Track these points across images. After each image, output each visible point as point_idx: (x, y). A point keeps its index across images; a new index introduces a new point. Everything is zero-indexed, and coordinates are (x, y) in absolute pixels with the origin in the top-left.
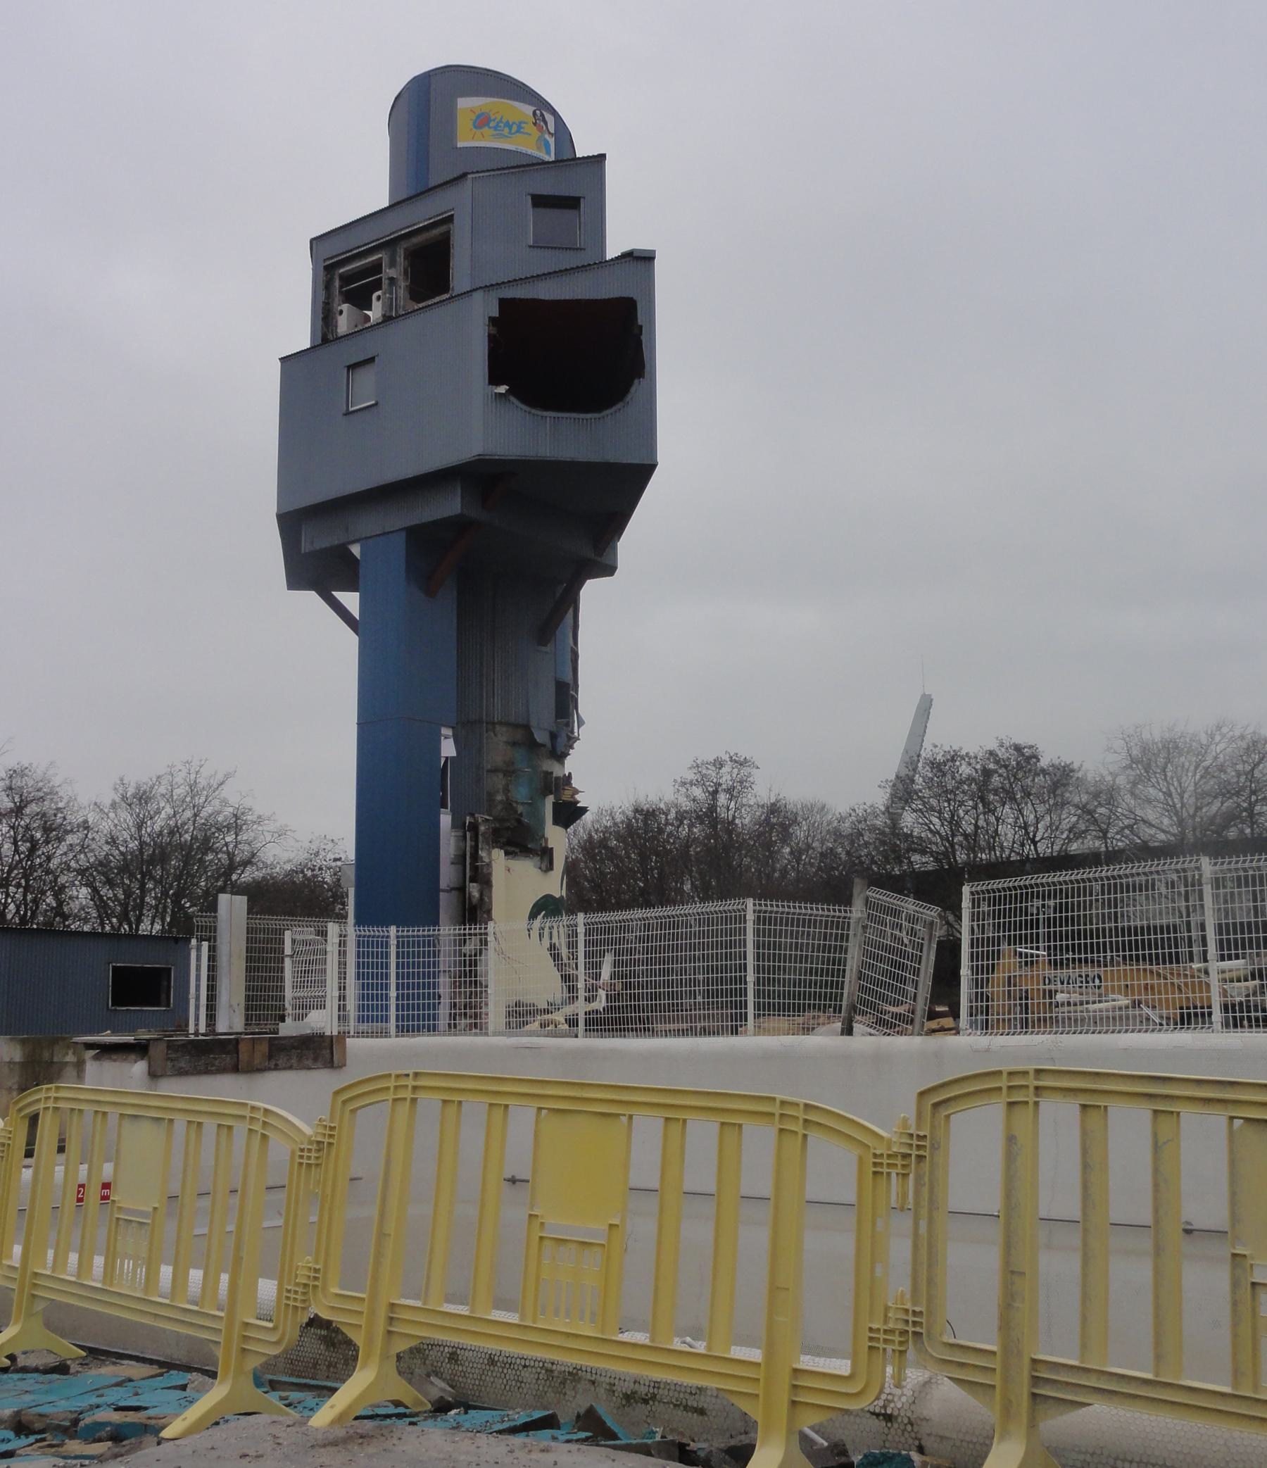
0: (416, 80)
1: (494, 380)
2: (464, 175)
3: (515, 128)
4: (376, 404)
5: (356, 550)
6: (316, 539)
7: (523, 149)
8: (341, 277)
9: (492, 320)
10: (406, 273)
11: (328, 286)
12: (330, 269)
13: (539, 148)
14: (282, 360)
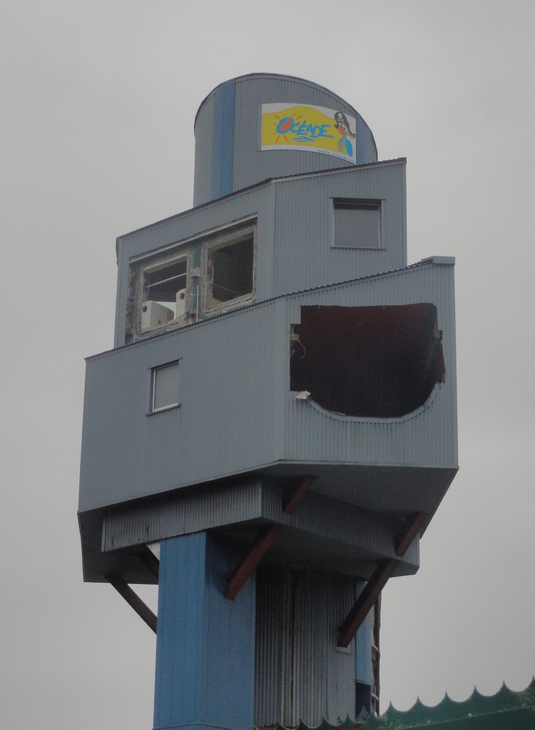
0: (222, 88)
1: (296, 386)
2: (269, 180)
3: (317, 131)
4: (179, 406)
5: (156, 550)
6: (117, 538)
7: (326, 151)
8: (146, 275)
9: (296, 328)
10: (209, 272)
11: (133, 284)
12: (135, 266)
13: (340, 150)
14: (88, 359)
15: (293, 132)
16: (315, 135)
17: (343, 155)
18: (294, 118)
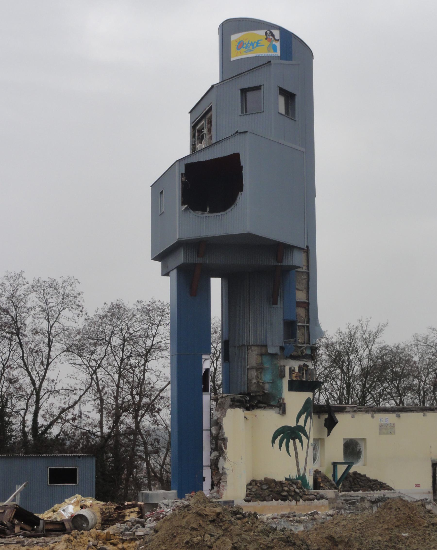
13: (269, 51)
15: (244, 48)
17: (271, 54)
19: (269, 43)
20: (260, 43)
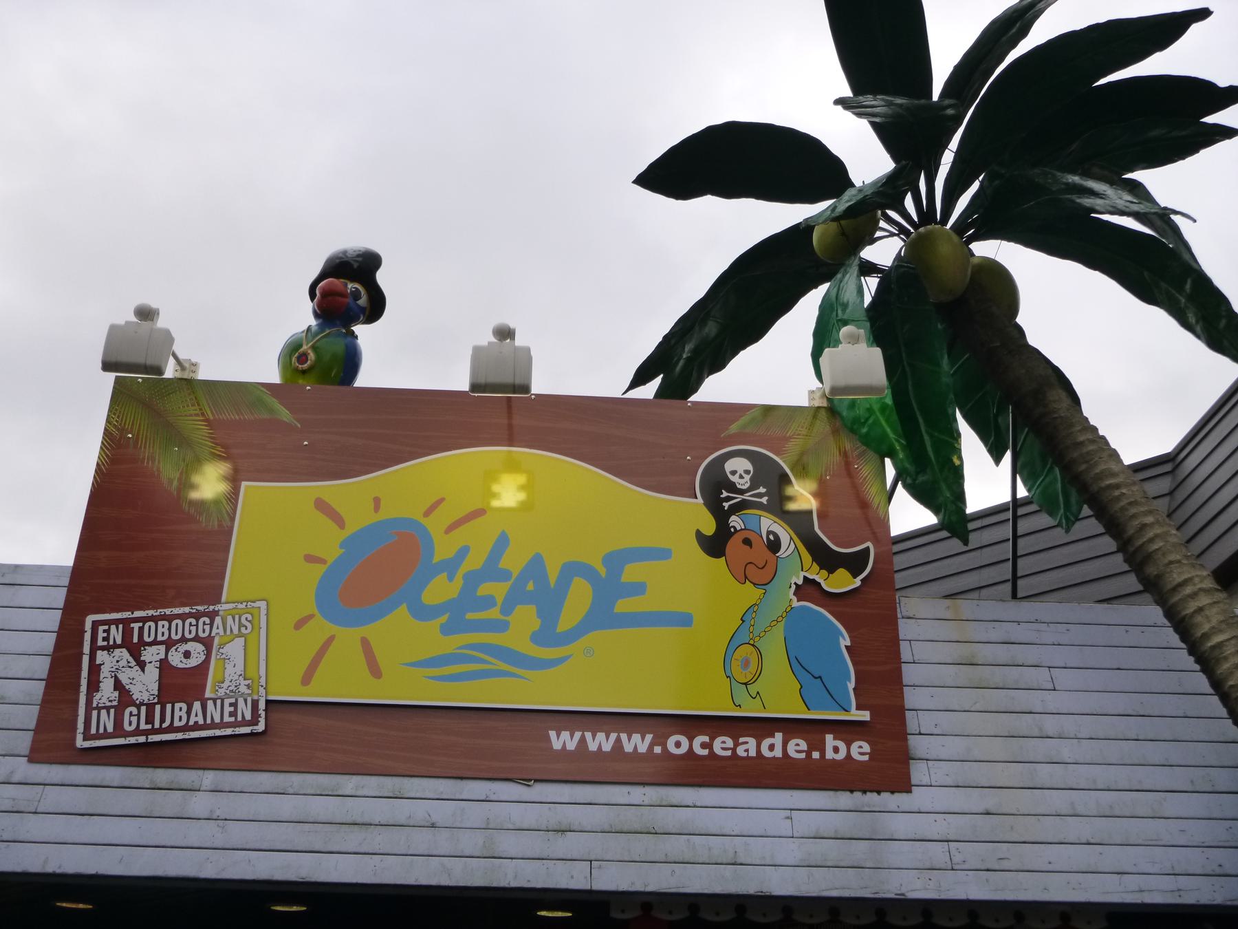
3: (580, 597)
15: (422, 613)
16: (568, 619)
18: (435, 525)
19: (750, 593)
20: (638, 589)
